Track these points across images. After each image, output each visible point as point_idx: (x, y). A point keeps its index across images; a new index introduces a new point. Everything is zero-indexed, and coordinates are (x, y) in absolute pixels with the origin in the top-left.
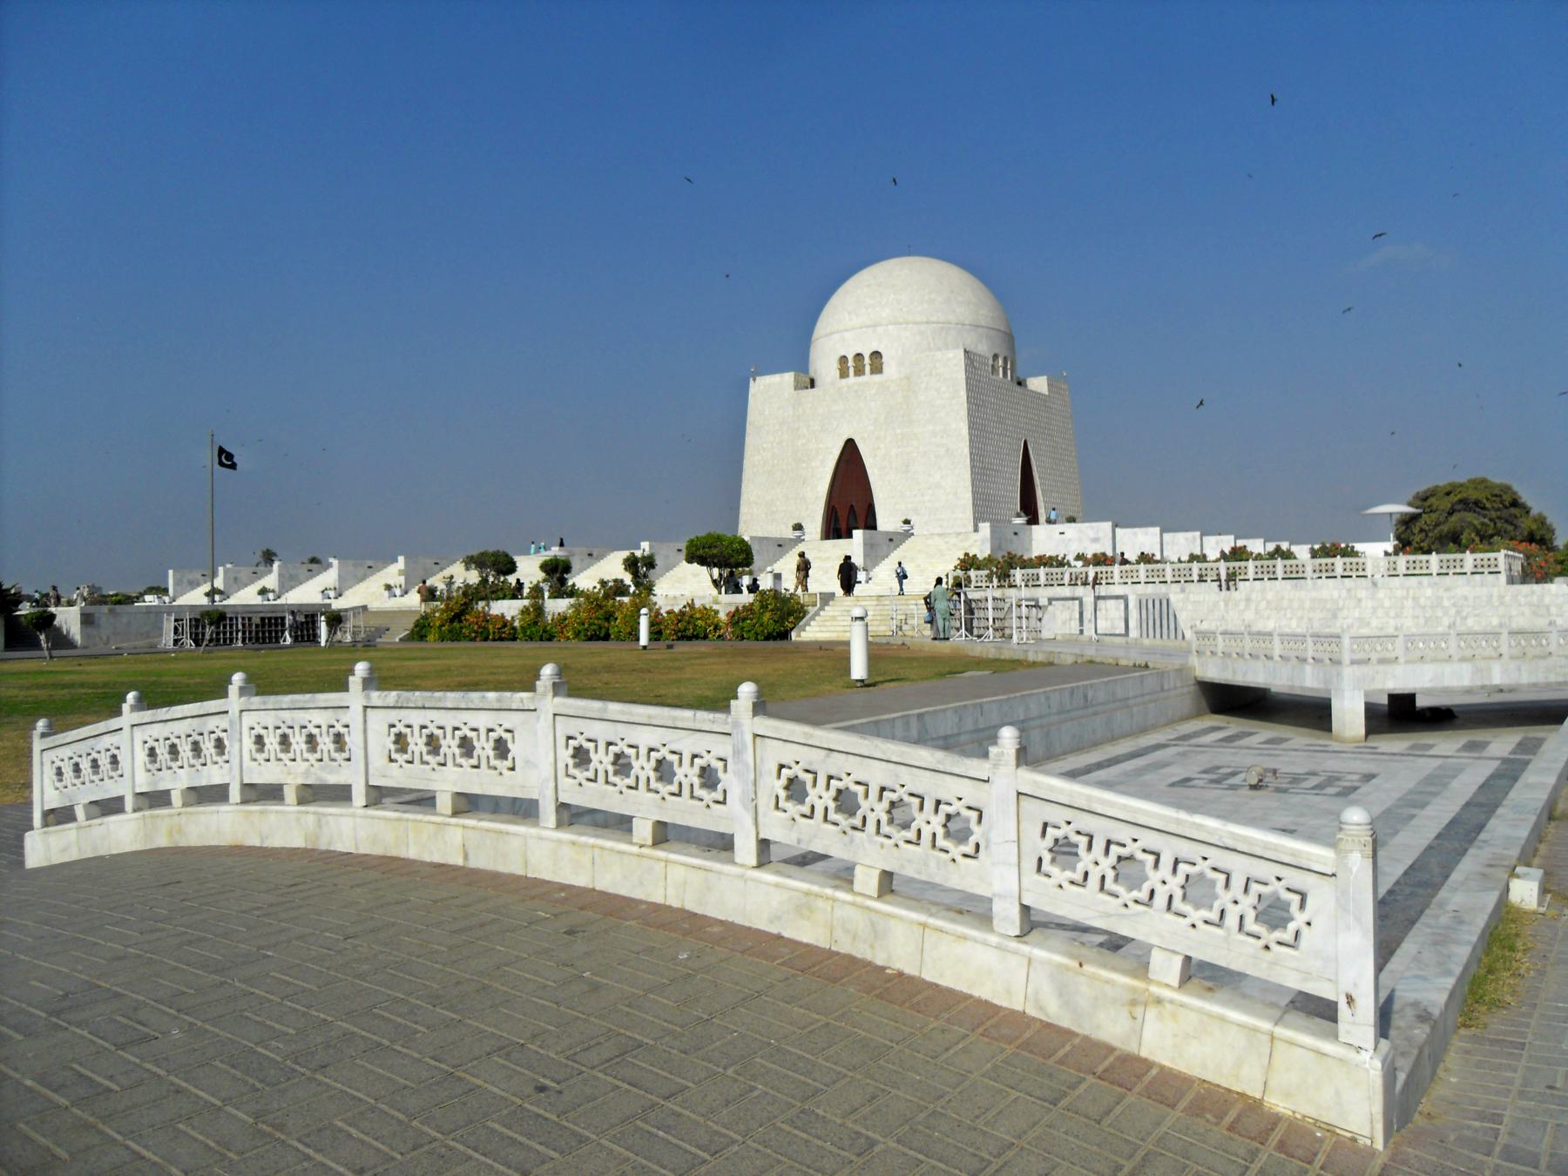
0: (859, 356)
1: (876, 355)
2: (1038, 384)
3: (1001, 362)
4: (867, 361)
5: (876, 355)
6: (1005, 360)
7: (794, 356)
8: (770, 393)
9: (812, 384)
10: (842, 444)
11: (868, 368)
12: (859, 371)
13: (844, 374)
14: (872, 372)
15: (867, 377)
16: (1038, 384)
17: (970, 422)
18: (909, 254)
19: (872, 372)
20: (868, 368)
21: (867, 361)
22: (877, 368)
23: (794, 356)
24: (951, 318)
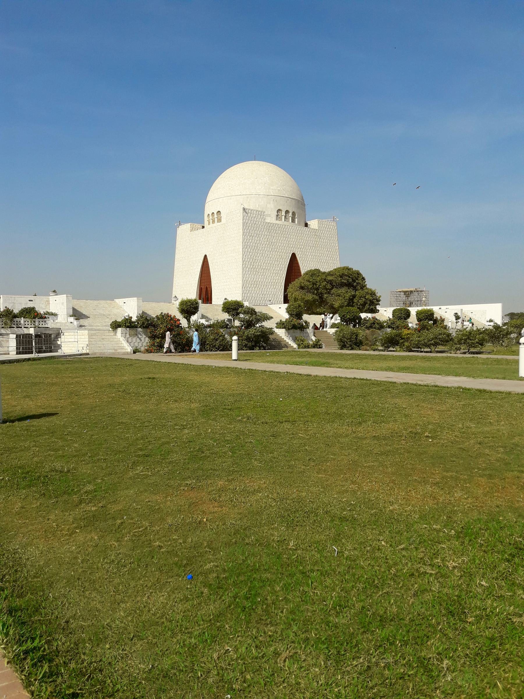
2: (313, 224)
3: (283, 213)
4: (216, 216)
6: (287, 212)
7: (196, 215)
8: (184, 231)
9: (203, 227)
12: (213, 222)
13: (209, 224)
14: (218, 222)
15: (216, 224)
19: (218, 222)
20: (216, 219)
22: (219, 220)
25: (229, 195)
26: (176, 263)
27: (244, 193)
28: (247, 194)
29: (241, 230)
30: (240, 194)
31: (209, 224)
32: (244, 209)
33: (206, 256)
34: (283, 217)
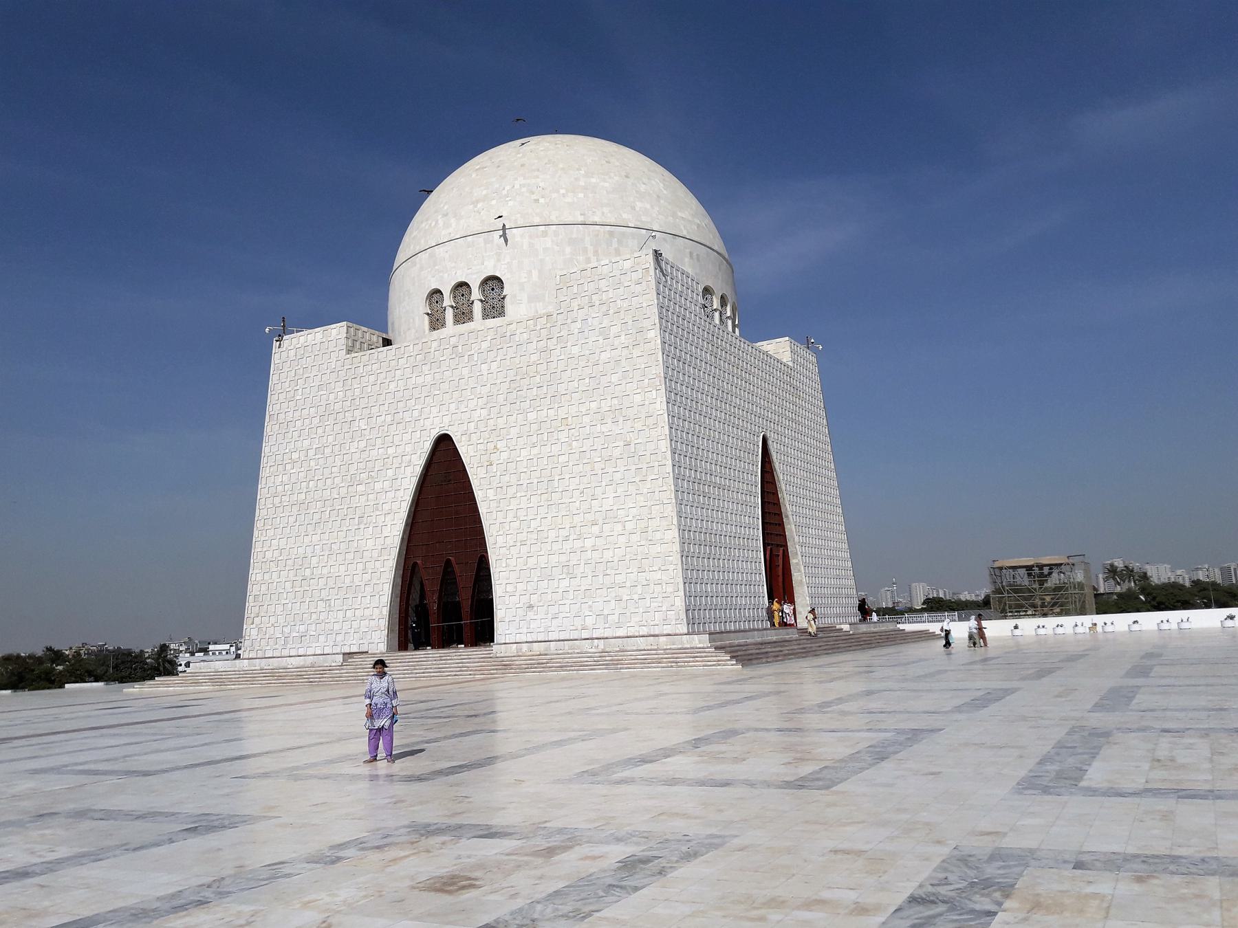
0: (462, 285)
1: (493, 282)
4: (476, 294)
5: (493, 282)
10: (428, 446)
11: (477, 308)
12: (463, 316)
13: (436, 322)
14: (486, 316)
16: (780, 348)
17: (669, 391)
18: (556, 132)
19: (486, 316)
20: (477, 308)
21: (476, 294)
22: (495, 308)
23: (362, 303)
24: (628, 217)
25: (537, 221)
26: (264, 473)
27: (597, 219)
28: (608, 221)
29: (654, 335)
30: (580, 219)
31: (436, 322)
32: (657, 255)
33: (444, 444)
34: (717, 315)
